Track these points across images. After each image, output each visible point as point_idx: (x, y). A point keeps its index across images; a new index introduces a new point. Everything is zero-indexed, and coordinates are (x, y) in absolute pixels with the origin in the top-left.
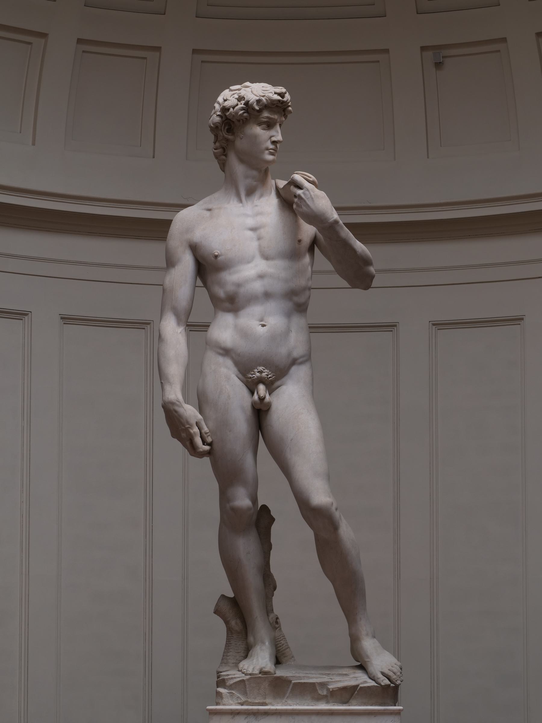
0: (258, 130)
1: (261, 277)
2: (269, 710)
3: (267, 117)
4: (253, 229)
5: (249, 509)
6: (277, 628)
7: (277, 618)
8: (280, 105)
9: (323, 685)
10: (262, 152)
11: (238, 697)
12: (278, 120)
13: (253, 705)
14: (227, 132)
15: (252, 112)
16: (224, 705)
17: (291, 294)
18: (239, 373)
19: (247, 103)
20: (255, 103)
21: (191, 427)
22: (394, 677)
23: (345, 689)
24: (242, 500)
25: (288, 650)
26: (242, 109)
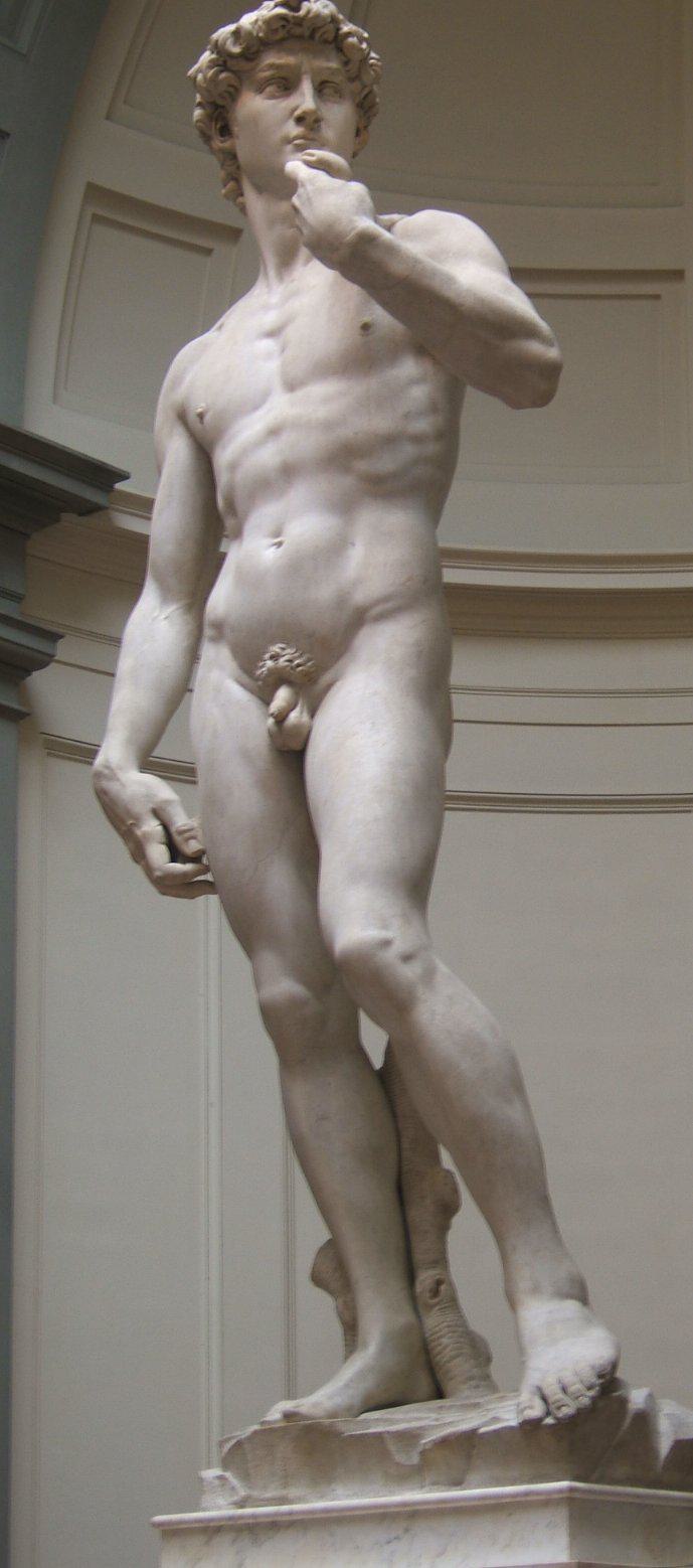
0: (255, 105)
1: (274, 432)
2: (276, 1514)
3: (271, 66)
4: (273, 334)
5: (294, 1003)
6: (432, 1307)
7: (439, 1283)
8: (298, 31)
9: (408, 1438)
10: (279, 152)
11: (233, 1489)
12: (305, 67)
13: (266, 1505)
14: (222, 136)
15: (240, 67)
16: (204, 1510)
17: (342, 456)
18: (239, 672)
19: (218, 48)
20: (229, 42)
21: (138, 820)
22: (555, 1394)
23: (444, 1442)
24: (284, 987)
25: (457, 1360)
26: (212, 64)
